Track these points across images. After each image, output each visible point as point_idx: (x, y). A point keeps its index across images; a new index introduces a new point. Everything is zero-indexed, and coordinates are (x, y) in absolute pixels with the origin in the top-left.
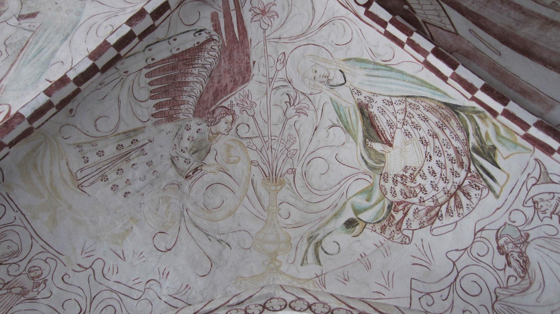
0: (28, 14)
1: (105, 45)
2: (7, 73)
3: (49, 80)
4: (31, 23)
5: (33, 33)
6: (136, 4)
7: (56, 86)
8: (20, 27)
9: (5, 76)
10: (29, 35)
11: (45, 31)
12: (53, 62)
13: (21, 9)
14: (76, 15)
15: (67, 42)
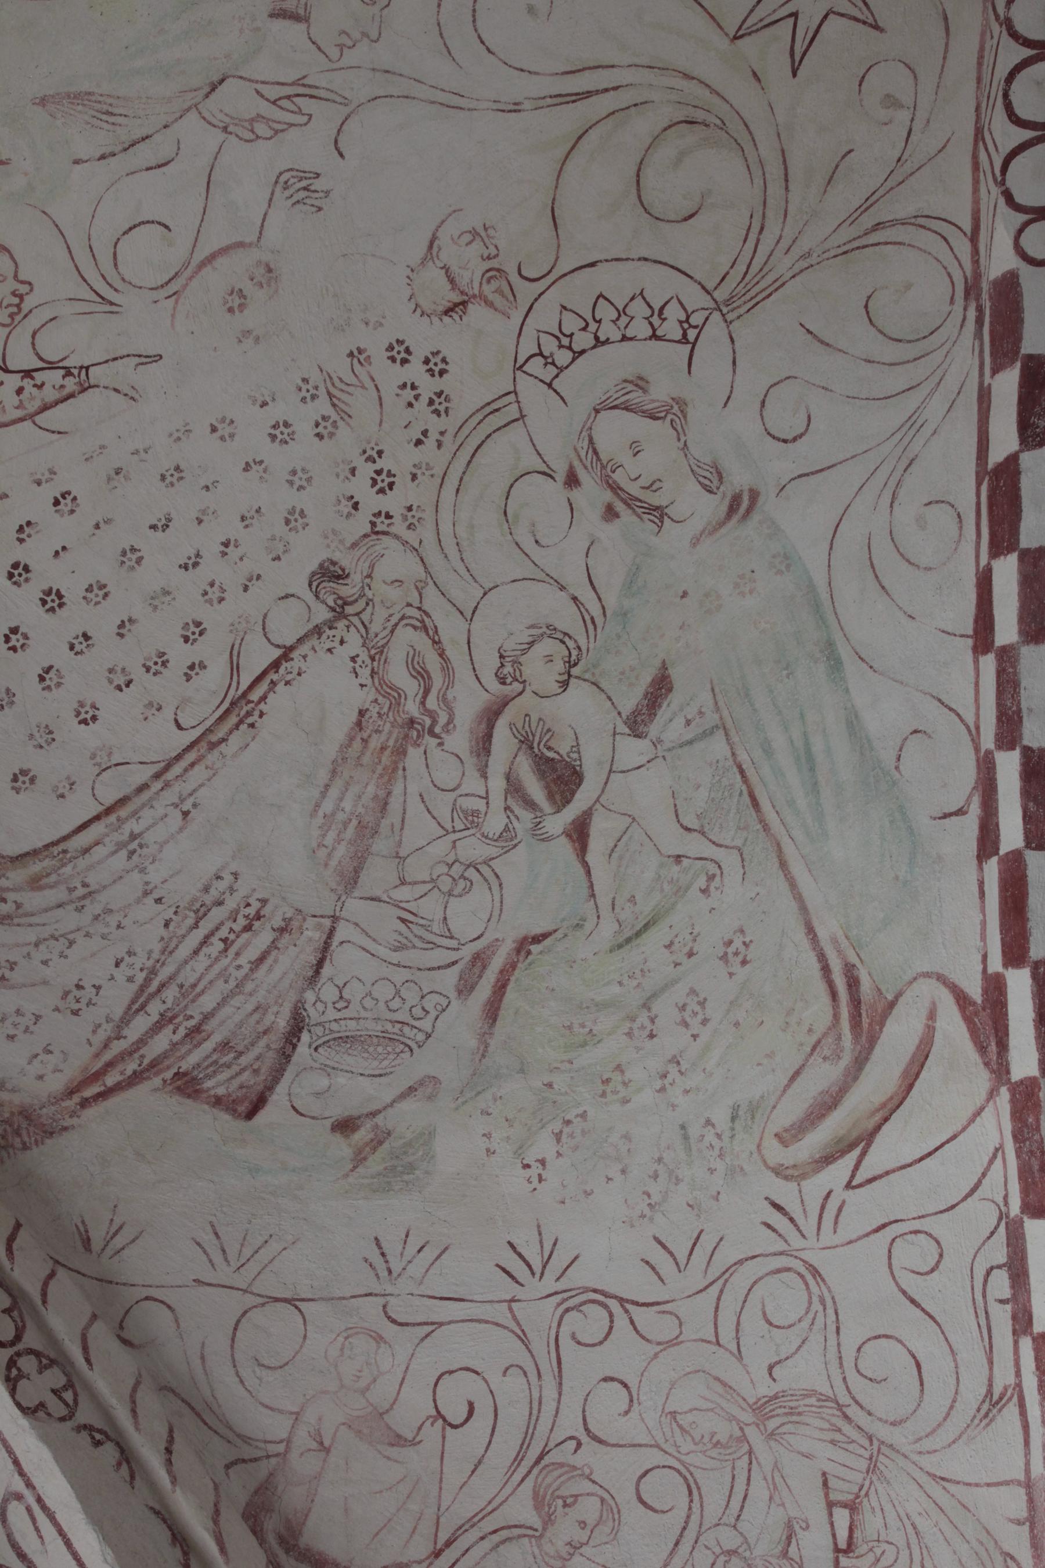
0: (646, 695)
1: (1035, 566)
2: (799, 898)
3: (947, 811)
4: (681, 710)
5: (721, 732)
6: (939, 372)
7: (1035, 800)
8: (669, 750)
9: (803, 909)
10: (718, 747)
11: (747, 695)
12: (888, 757)
13: (610, 698)
14: (780, 572)
15: (851, 667)
